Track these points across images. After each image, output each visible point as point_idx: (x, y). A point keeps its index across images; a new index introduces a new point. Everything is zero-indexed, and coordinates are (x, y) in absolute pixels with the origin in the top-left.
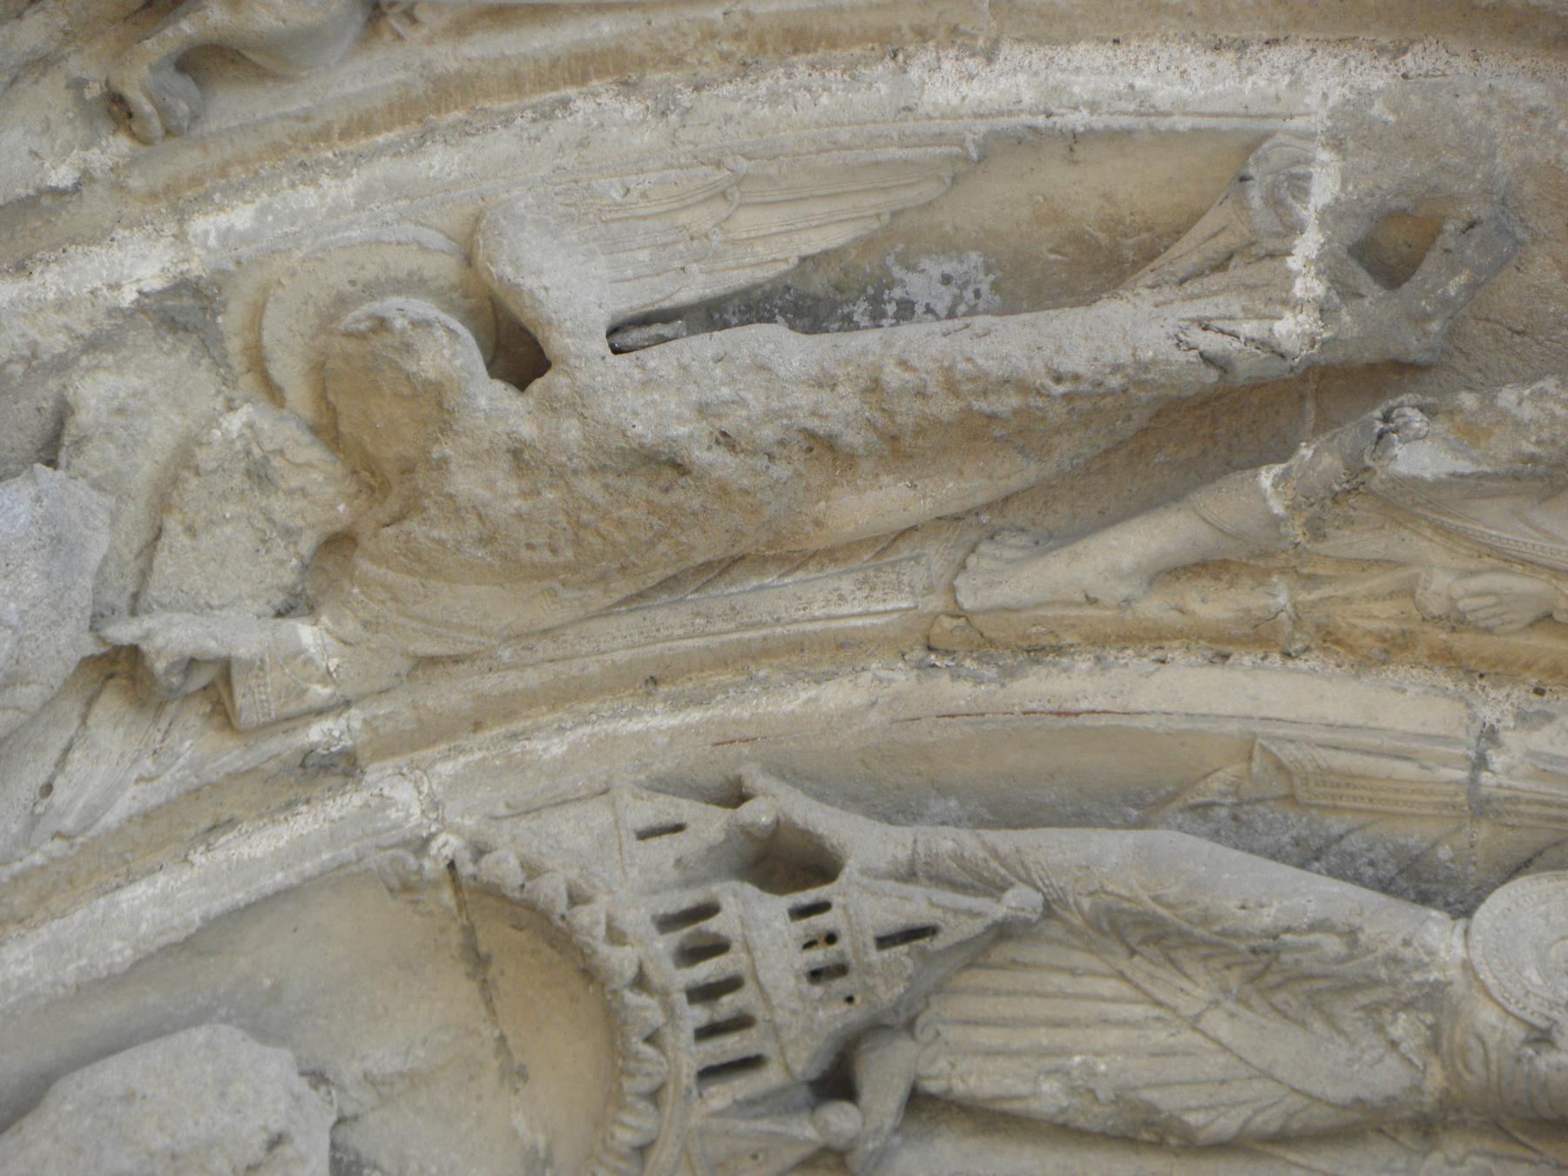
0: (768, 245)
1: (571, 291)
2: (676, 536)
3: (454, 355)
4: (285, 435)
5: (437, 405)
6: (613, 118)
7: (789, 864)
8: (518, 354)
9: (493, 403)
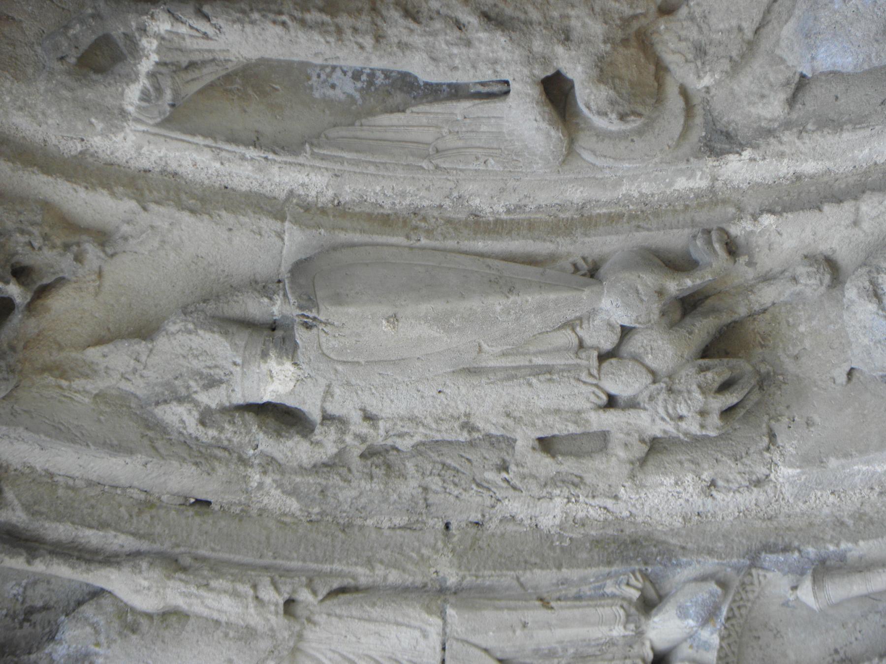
0: (419, 122)
1: (522, 118)
3: (588, 95)
4: (682, 72)
5: (604, 72)
6: (485, 200)
8: (556, 92)
9: (575, 69)
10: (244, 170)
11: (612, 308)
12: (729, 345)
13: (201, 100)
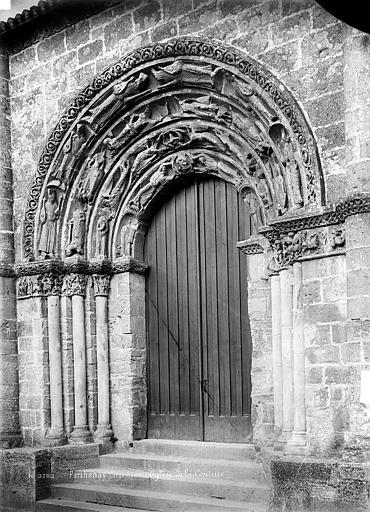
1: (107, 195)
2: (120, 199)
7: (132, 203)
8: (108, 198)
10: (113, 171)
11: (89, 194)
12: (83, 201)
13: (119, 171)
